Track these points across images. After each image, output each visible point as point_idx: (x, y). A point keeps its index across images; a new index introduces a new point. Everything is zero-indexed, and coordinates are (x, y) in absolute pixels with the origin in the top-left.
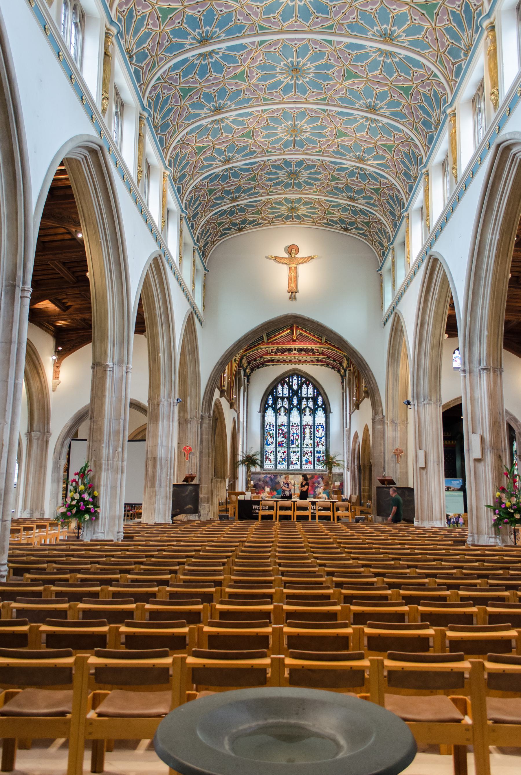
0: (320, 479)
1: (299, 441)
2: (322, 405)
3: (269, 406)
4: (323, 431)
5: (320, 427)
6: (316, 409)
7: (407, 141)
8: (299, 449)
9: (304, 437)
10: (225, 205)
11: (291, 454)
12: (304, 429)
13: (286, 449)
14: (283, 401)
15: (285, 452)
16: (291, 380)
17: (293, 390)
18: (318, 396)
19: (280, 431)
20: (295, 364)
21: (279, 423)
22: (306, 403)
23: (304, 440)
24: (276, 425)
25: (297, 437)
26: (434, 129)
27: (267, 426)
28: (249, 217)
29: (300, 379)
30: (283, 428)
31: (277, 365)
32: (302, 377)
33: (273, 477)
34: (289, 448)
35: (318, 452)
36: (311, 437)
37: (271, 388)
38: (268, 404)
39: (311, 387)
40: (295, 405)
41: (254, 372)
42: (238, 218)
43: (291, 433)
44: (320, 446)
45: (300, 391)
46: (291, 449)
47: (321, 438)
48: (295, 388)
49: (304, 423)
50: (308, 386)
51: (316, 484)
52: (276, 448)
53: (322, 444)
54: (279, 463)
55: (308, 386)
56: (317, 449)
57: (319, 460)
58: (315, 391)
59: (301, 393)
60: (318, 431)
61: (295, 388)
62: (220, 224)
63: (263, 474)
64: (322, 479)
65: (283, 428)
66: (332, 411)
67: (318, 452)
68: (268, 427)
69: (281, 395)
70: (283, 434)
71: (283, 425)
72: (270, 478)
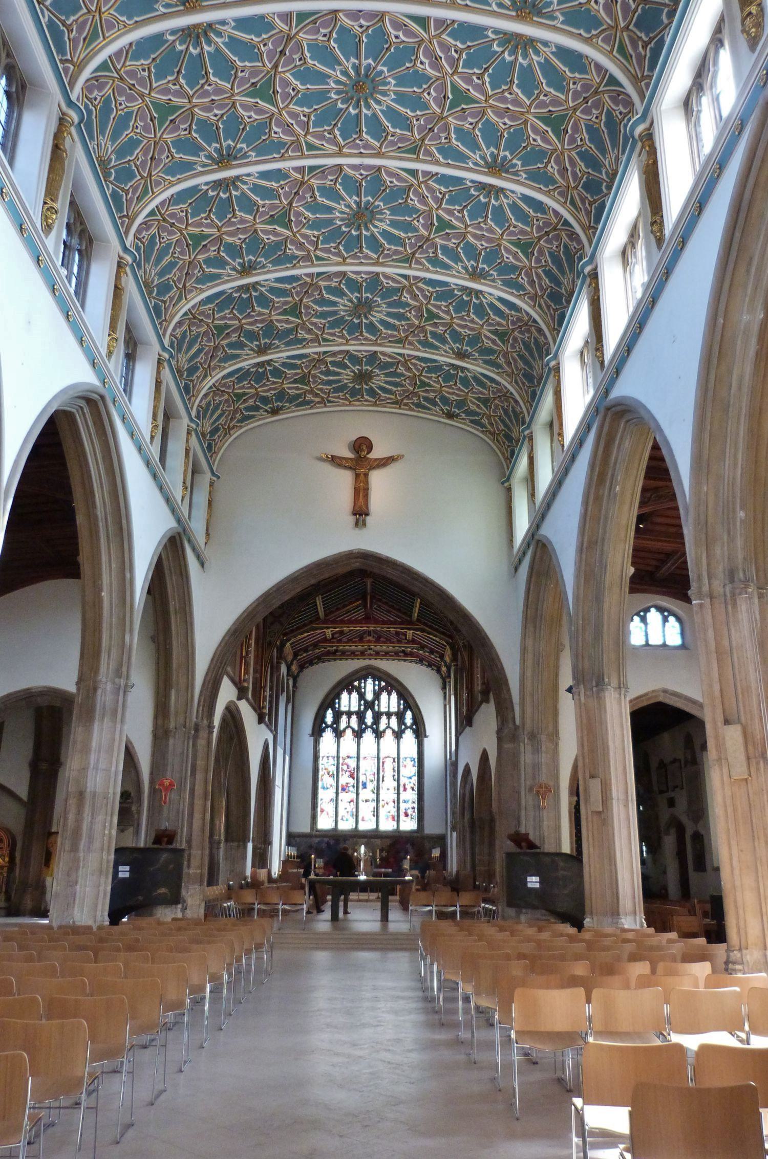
0: (409, 846)
1: (375, 783)
2: (412, 725)
3: (327, 726)
4: (414, 766)
5: (408, 760)
6: (403, 732)
7: (527, 325)
8: (374, 796)
9: (383, 777)
10: (245, 360)
11: (361, 804)
12: (383, 763)
13: (354, 796)
14: (349, 717)
15: (352, 801)
16: (363, 685)
17: (366, 702)
18: (405, 710)
19: (345, 767)
20: (370, 659)
21: (343, 754)
22: (386, 721)
23: (383, 781)
24: (338, 758)
25: (372, 777)
26: (565, 304)
27: (323, 757)
28: (289, 388)
29: (377, 683)
30: (348, 761)
31: (341, 659)
32: (380, 680)
33: (332, 842)
34: (357, 794)
35: (405, 802)
36: (394, 776)
37: (332, 696)
38: (326, 723)
39: (394, 696)
40: (369, 724)
41: (305, 671)
42: (271, 389)
43: (362, 771)
44: (409, 790)
45: (377, 702)
46: (362, 797)
47: (410, 778)
48: (369, 696)
49: (382, 755)
50: (389, 694)
51: (402, 854)
52: (337, 793)
53: (413, 789)
54: (342, 819)
55: (389, 694)
56: (403, 797)
57: (406, 815)
58: (402, 702)
59: (379, 705)
60: (405, 766)
61: (369, 696)
62: (239, 396)
63: (316, 836)
64: (413, 845)
65: (348, 761)
66: (427, 734)
67: (405, 802)
68: (325, 758)
69: (346, 709)
70: (350, 771)
71: (348, 757)
72: (328, 843)
